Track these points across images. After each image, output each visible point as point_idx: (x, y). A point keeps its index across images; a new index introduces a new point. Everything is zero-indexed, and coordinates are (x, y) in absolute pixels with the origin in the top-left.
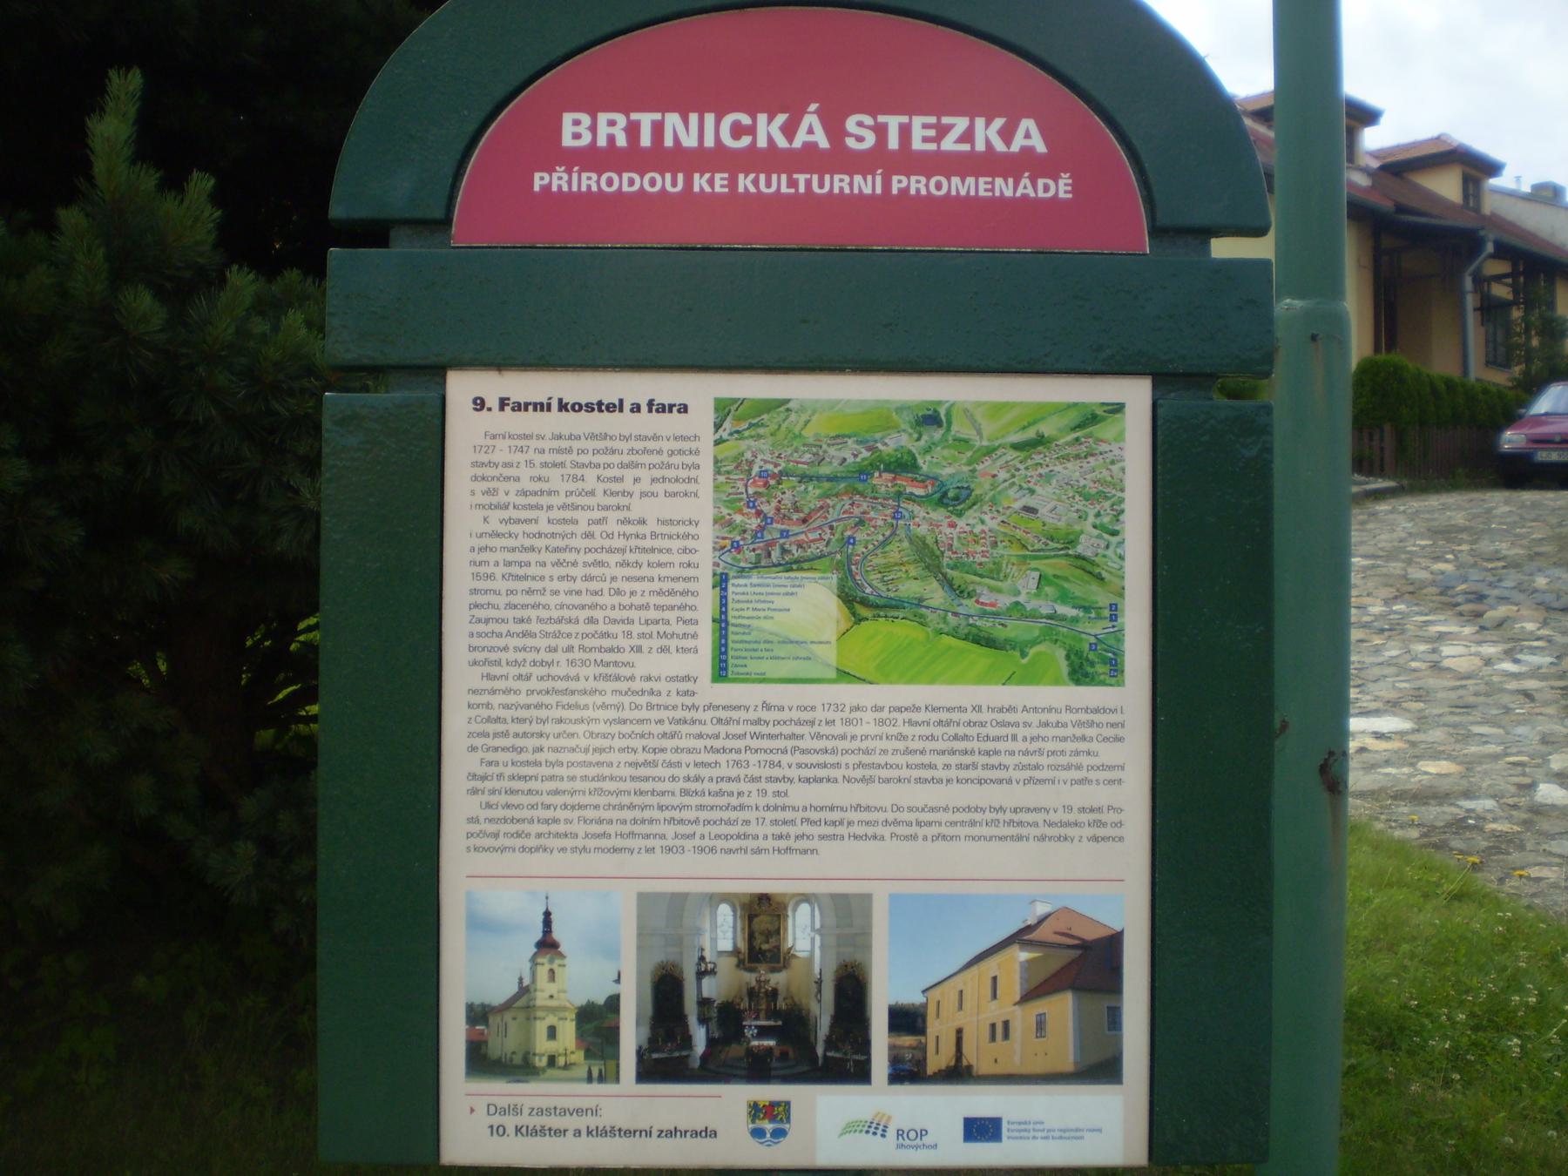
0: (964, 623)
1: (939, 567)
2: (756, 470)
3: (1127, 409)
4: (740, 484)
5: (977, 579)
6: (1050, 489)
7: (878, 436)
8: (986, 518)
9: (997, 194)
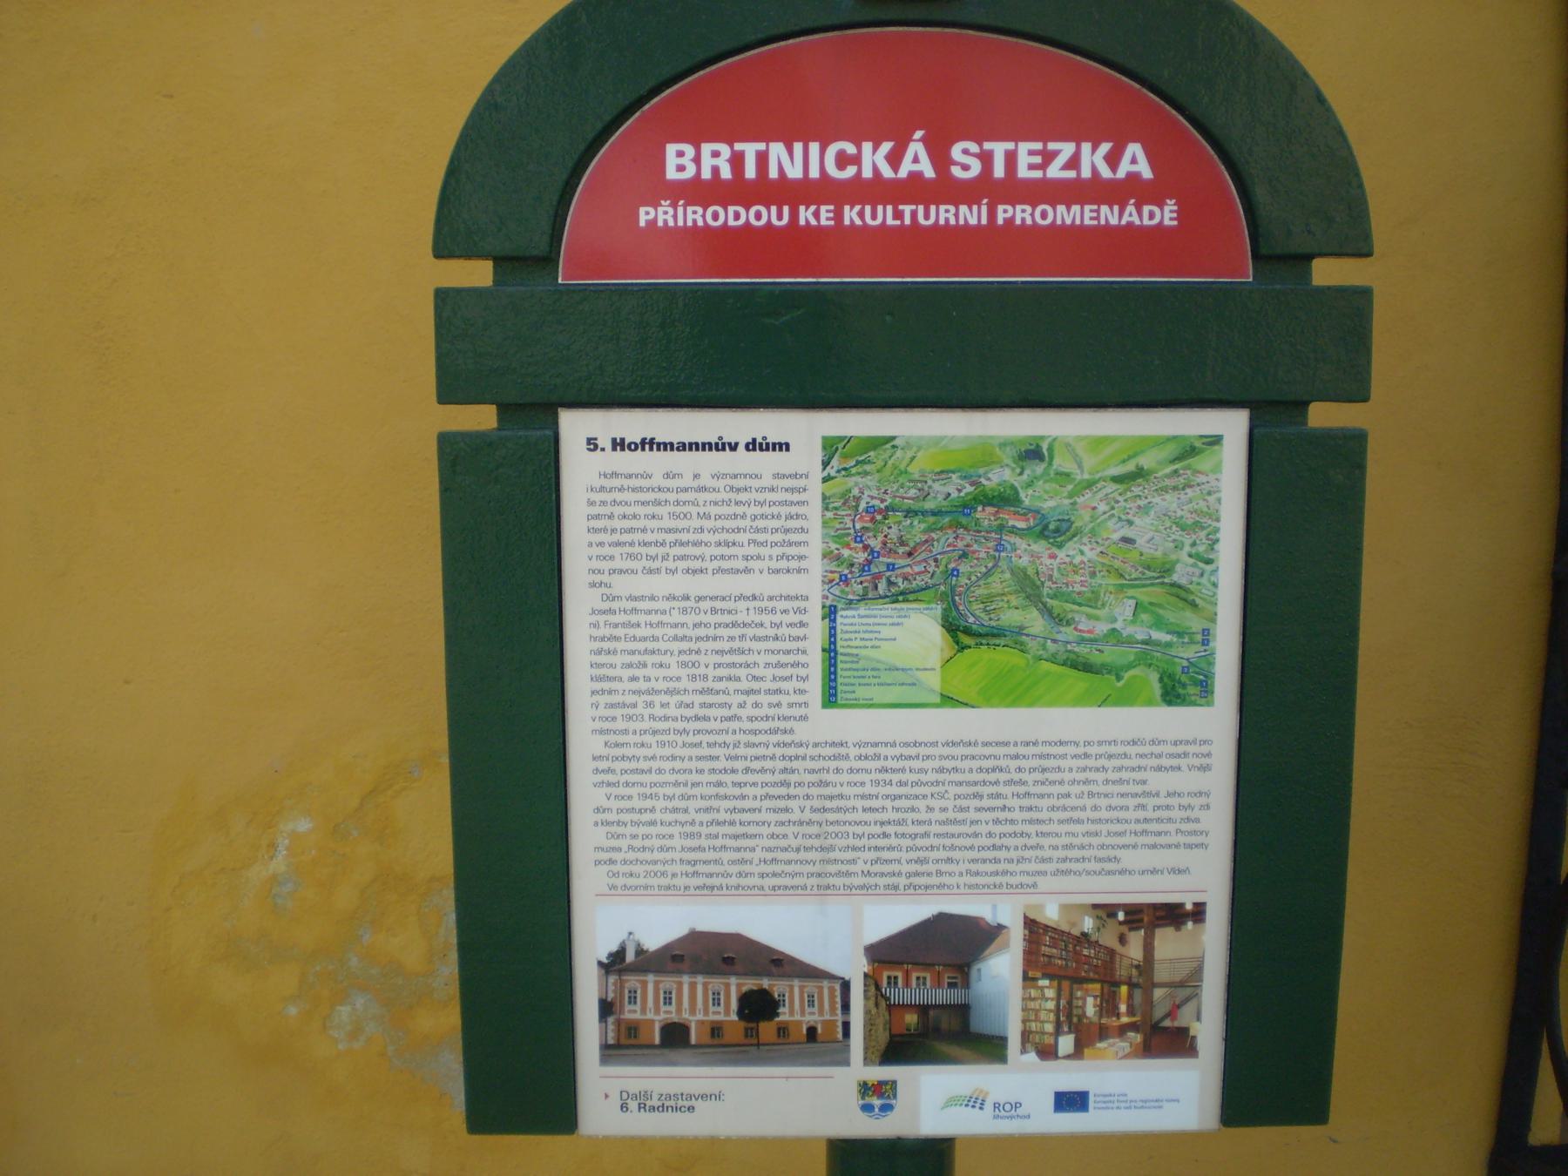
1: (1039, 596)
2: (863, 505)
3: (1225, 441)
4: (847, 520)
5: (1076, 607)
6: (1148, 520)
7: (981, 471)
8: (1086, 549)
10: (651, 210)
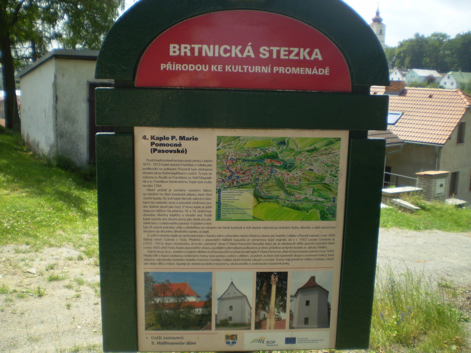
0: (290, 203)
1: (284, 187)
2: (229, 158)
3: (342, 140)
4: (225, 163)
7: (266, 148)
8: (298, 172)
9: (306, 73)
10: (165, 65)
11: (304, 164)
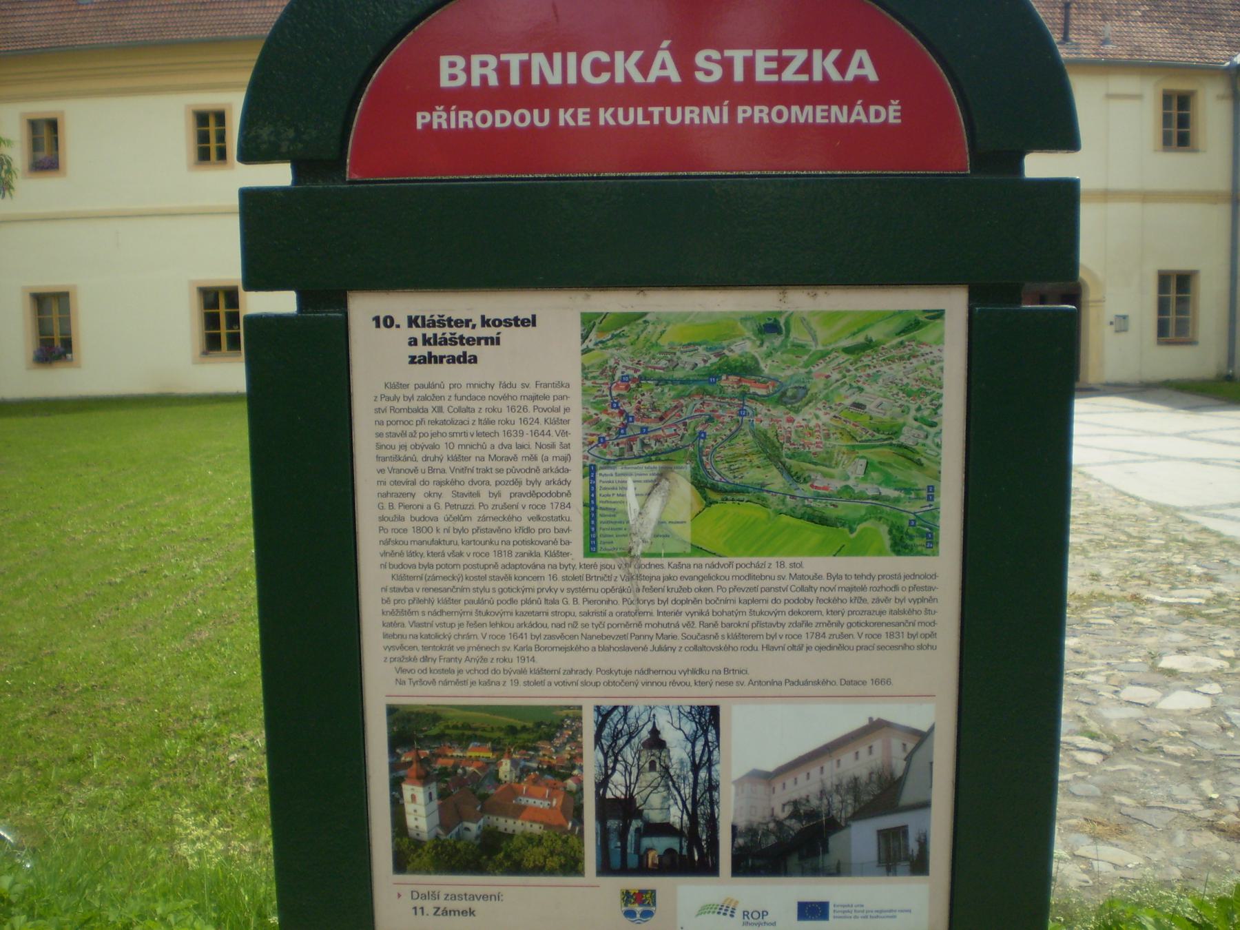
1: (779, 457)
2: (618, 375)
3: (946, 315)
4: (605, 388)
6: (876, 387)
7: (725, 343)
8: (820, 413)
9: (833, 120)
10: (427, 115)
11: (838, 388)
